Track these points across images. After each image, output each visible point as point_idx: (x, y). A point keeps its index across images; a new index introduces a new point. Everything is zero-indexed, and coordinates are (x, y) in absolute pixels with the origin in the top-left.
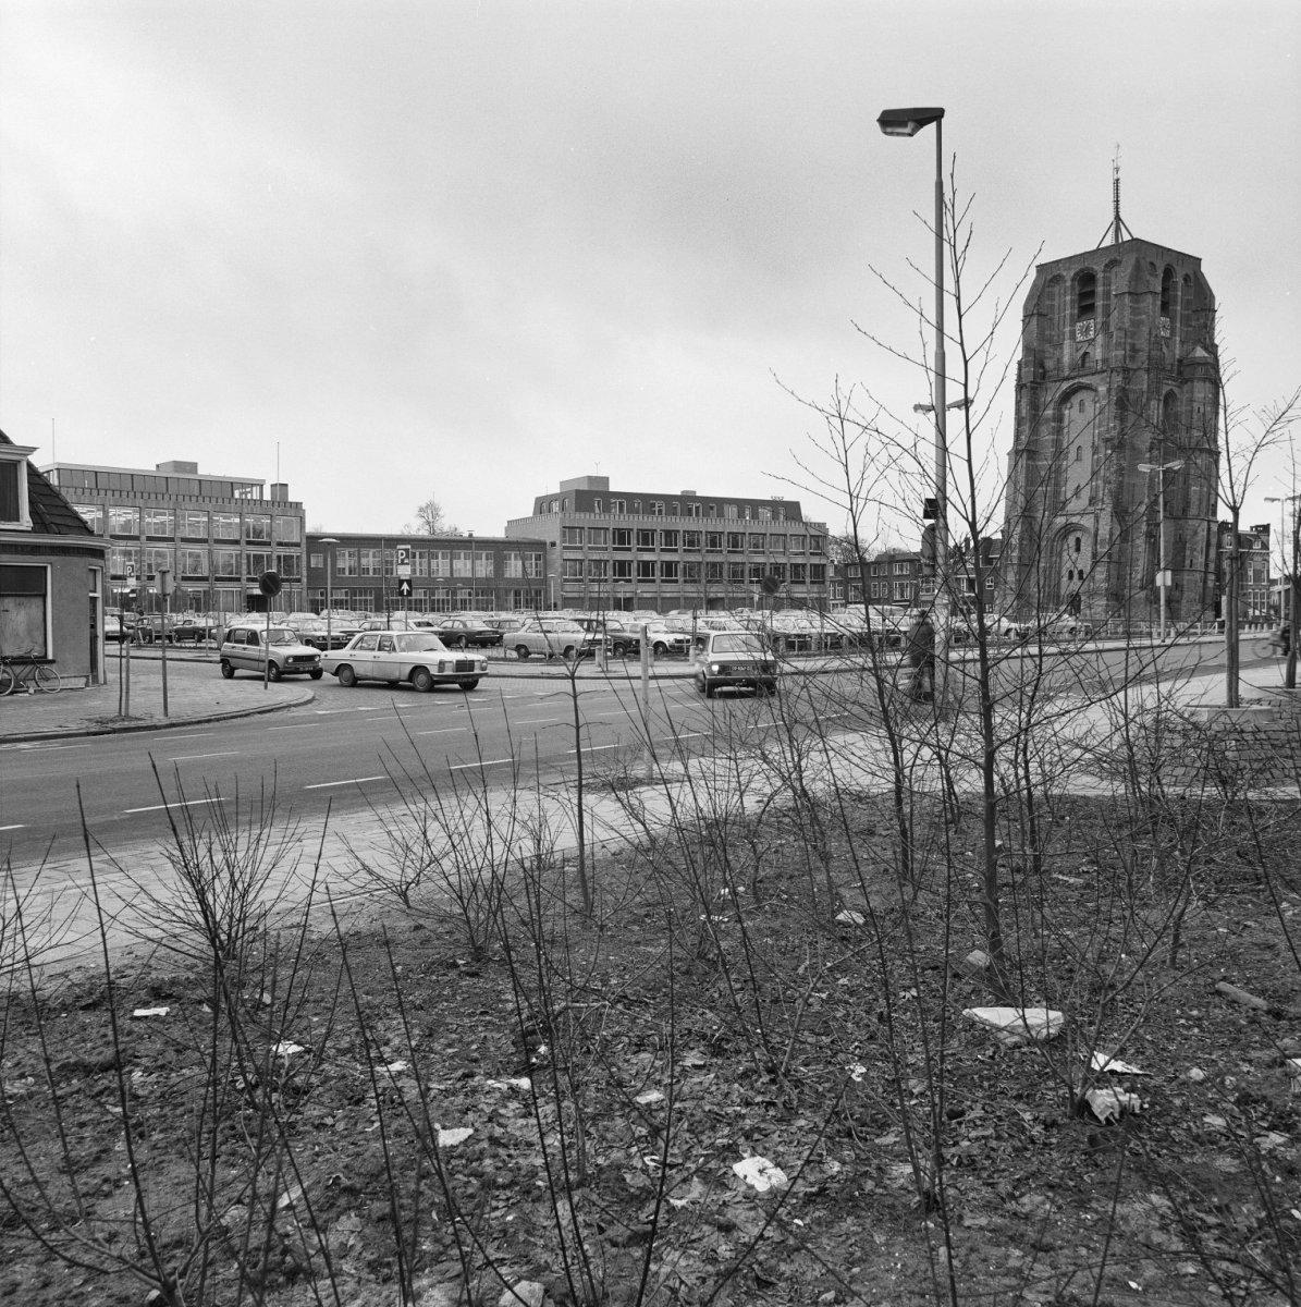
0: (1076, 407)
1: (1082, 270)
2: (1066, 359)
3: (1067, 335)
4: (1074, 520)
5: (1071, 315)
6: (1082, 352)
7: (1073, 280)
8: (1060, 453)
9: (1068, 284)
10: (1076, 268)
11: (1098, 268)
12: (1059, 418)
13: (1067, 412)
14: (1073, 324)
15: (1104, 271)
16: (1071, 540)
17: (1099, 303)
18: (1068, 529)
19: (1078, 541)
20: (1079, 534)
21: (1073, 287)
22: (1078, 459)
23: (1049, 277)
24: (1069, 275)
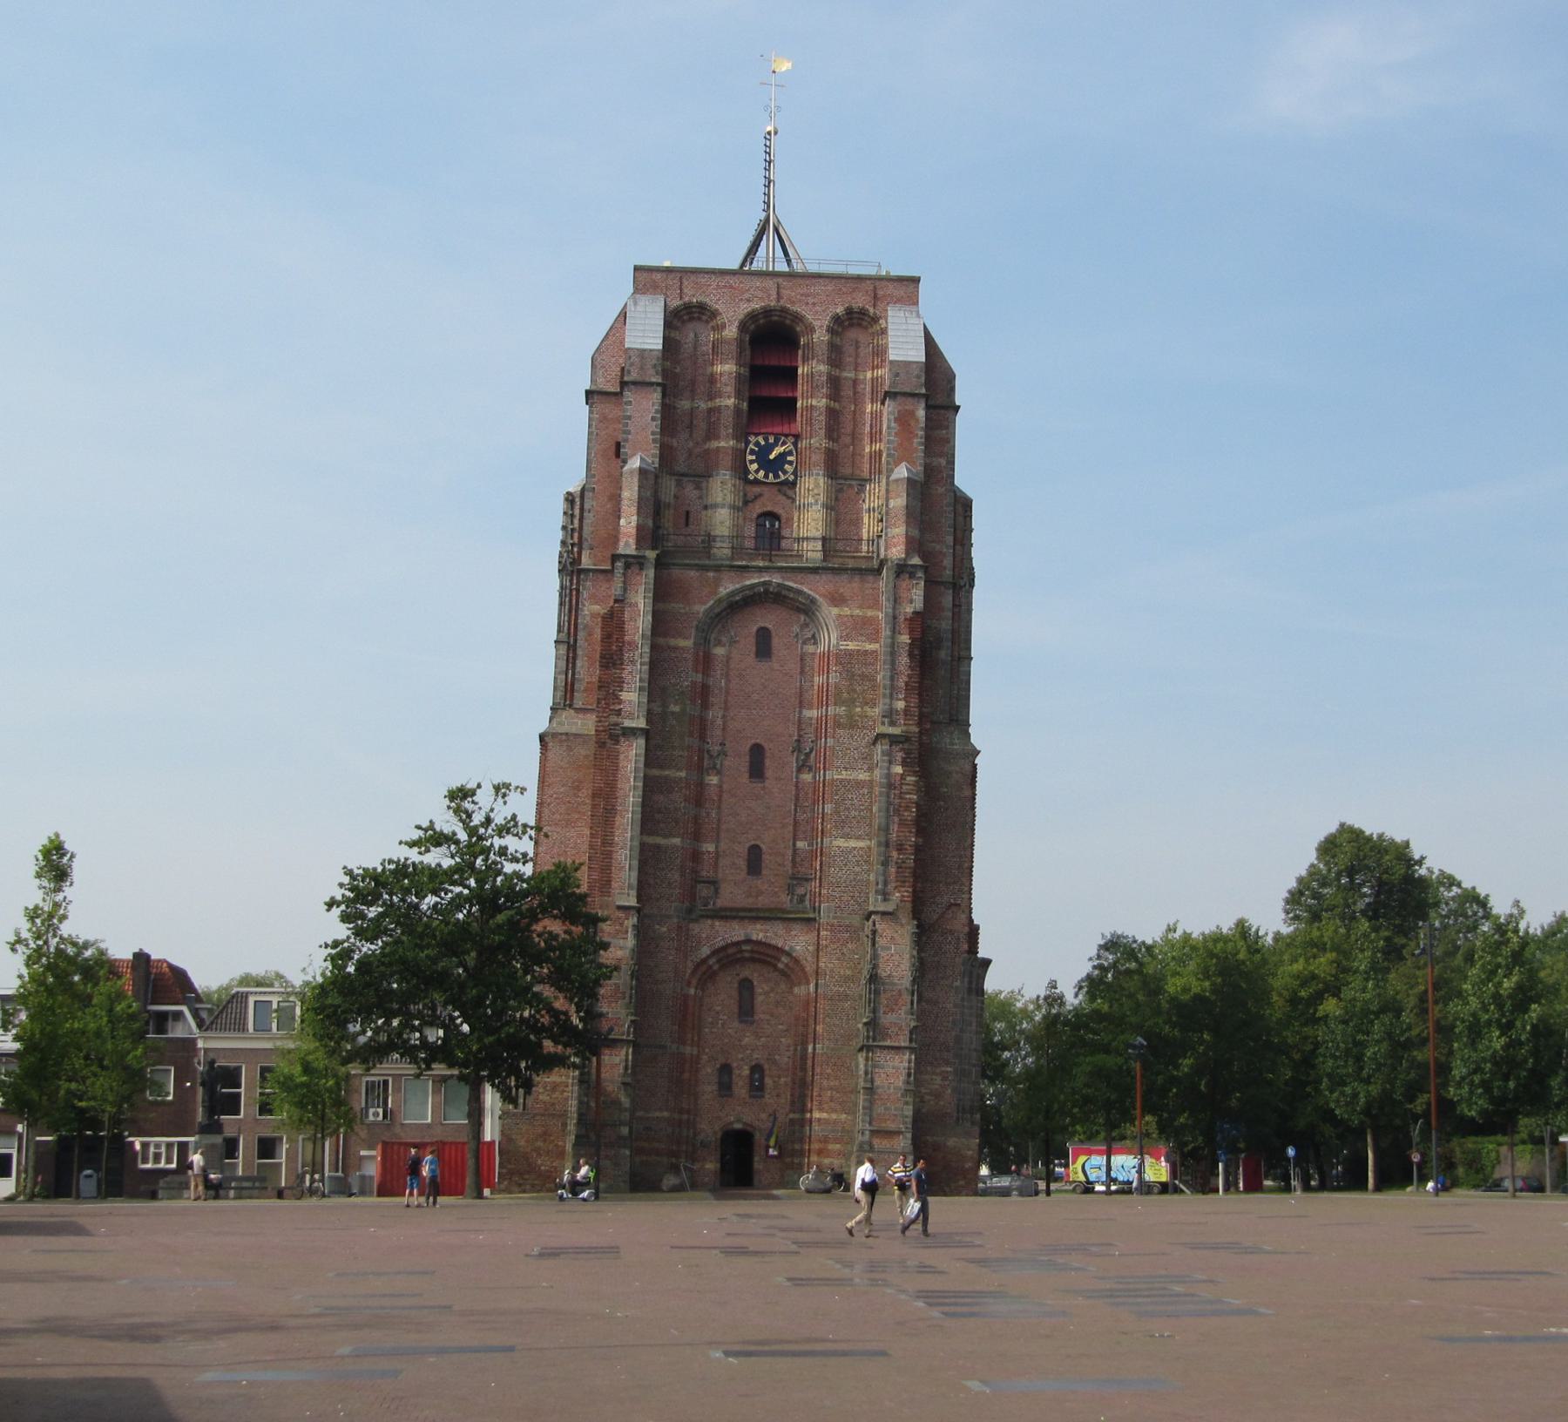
0: (748, 643)
1: (767, 312)
2: (722, 521)
3: (727, 460)
4: (758, 932)
5: (737, 411)
6: (758, 508)
7: (743, 327)
8: (702, 763)
9: (731, 332)
10: (756, 300)
11: (817, 320)
12: (705, 662)
13: (719, 651)
14: (742, 434)
15: (831, 331)
16: (723, 996)
17: (812, 401)
18: (730, 956)
19: (746, 986)
20: (746, 972)
21: (740, 342)
22: (757, 770)
23: (675, 303)
24: (732, 315)
